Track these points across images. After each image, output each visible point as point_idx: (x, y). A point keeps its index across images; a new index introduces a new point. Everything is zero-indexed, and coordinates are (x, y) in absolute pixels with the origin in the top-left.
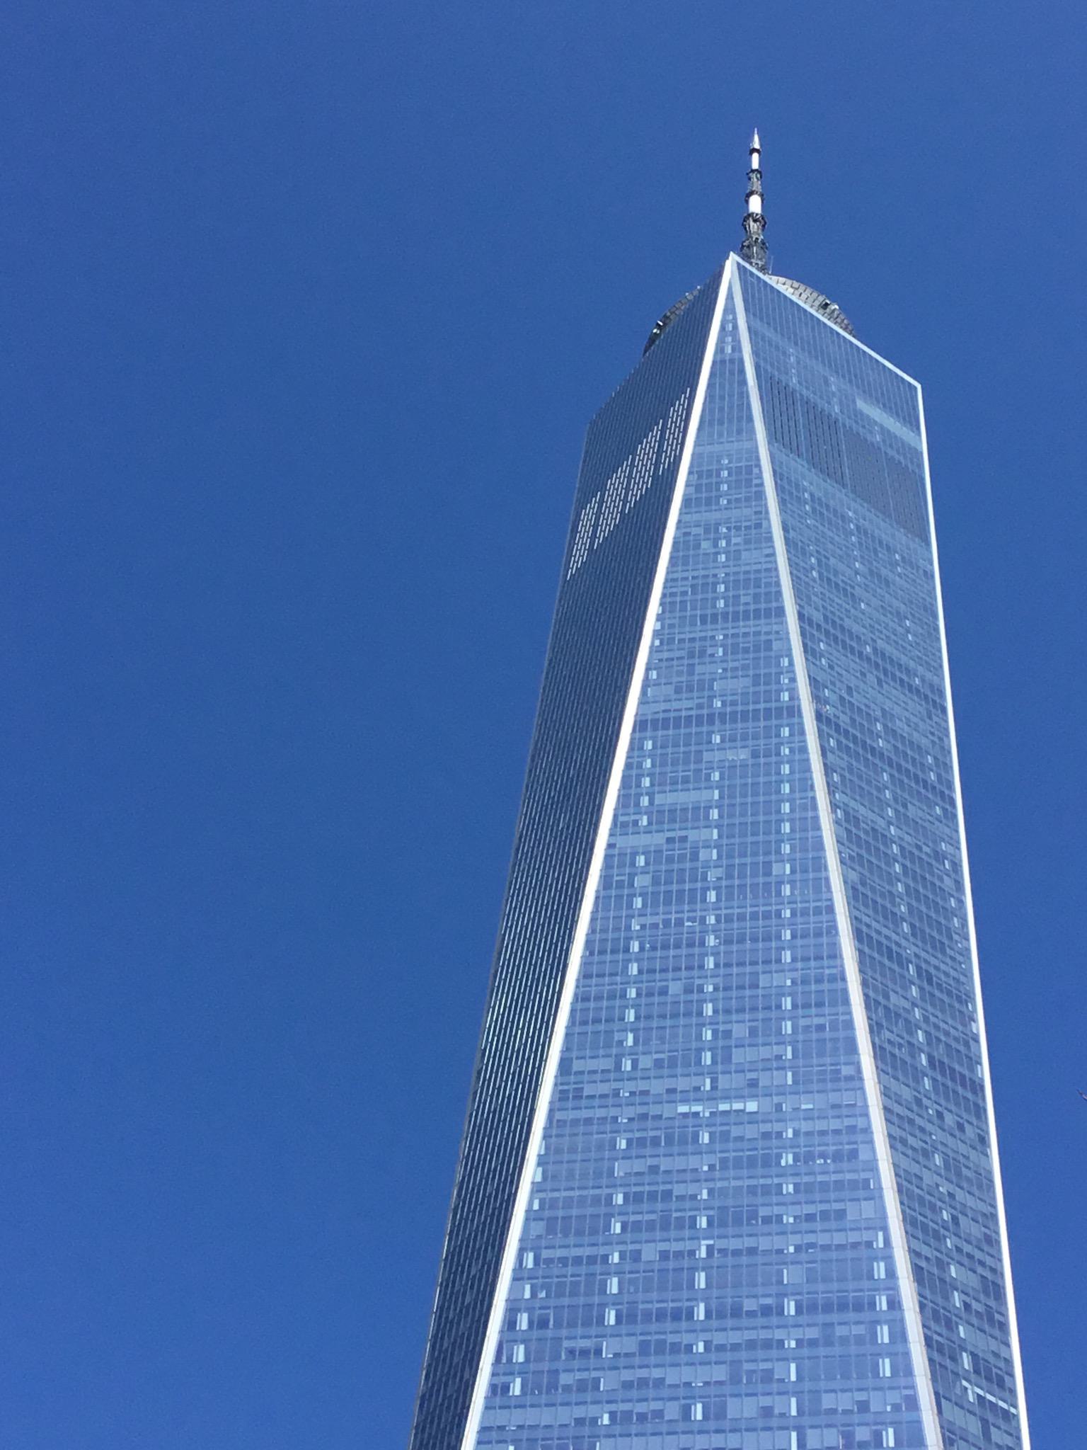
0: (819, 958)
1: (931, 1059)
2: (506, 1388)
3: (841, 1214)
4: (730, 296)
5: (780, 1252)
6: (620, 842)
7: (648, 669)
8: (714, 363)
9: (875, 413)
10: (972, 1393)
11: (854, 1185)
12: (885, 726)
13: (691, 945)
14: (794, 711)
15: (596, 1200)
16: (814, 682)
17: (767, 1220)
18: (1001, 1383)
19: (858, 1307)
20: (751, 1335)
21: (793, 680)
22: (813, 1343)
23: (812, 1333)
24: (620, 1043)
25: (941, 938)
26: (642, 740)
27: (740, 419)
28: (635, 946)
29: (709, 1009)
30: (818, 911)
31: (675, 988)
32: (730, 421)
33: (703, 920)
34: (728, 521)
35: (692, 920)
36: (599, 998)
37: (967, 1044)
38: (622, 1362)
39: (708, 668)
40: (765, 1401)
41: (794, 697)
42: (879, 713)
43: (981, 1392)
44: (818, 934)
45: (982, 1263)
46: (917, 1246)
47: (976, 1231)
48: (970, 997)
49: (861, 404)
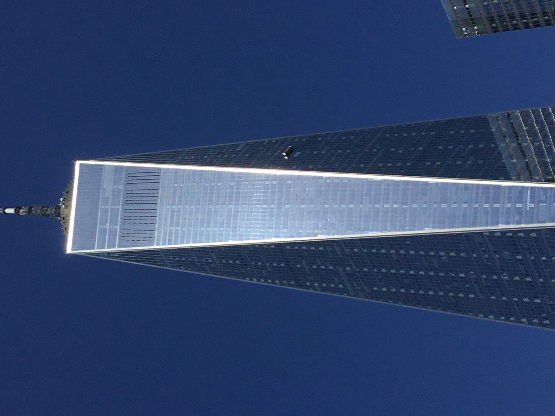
3: (480, 243)
7: (276, 284)
26: (306, 286)
30: (362, 243)
35: (377, 276)
43: (528, 202)
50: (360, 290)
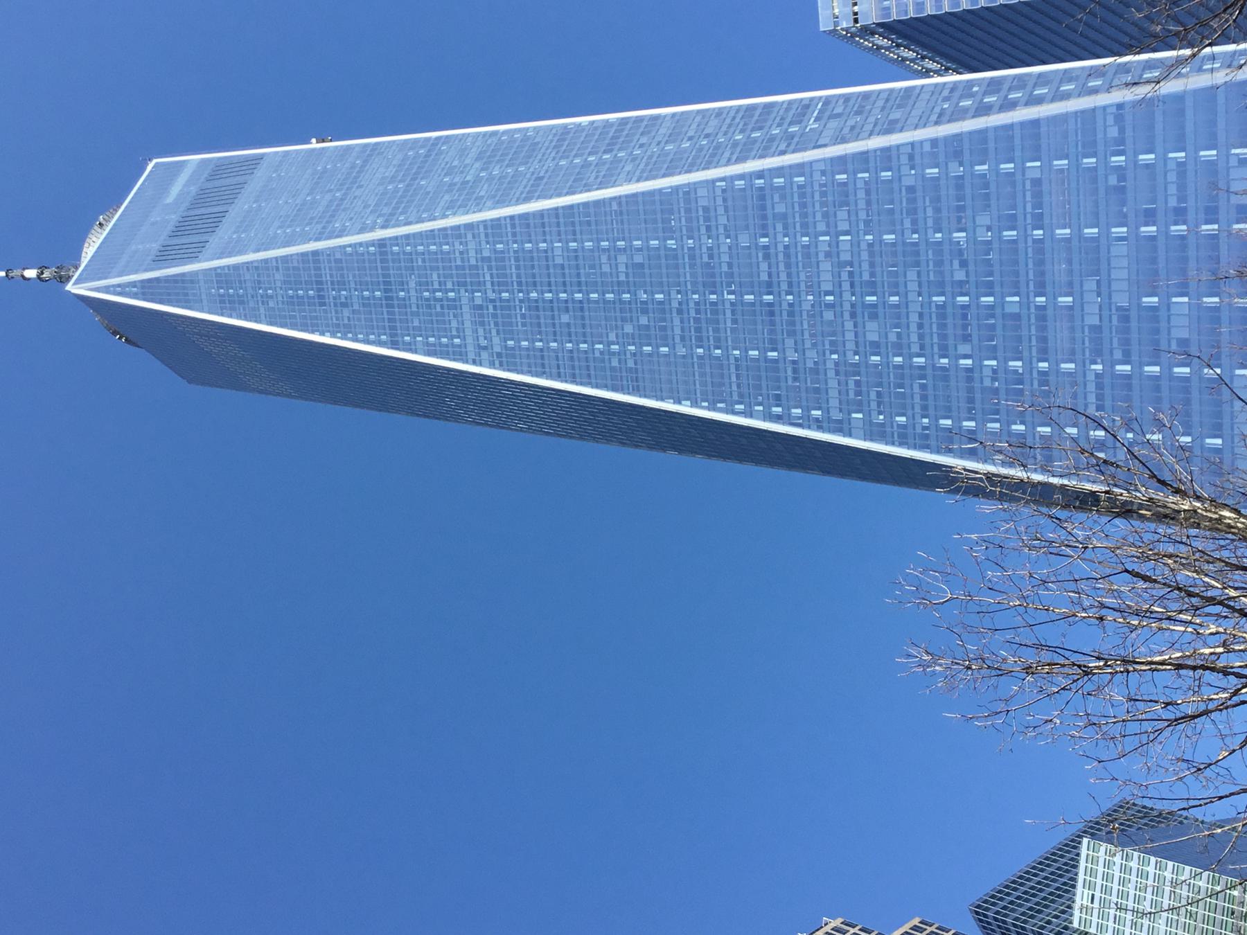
0: (543, 225)
1: (605, 152)
2: (817, 420)
3: (706, 209)
4: (97, 290)
5: (730, 248)
6: (471, 356)
8: (145, 300)
9: (175, 190)
10: (812, 125)
11: (687, 201)
12: (390, 183)
13: (537, 308)
14: (381, 243)
15: (701, 366)
16: (362, 230)
17: (711, 257)
18: (807, 107)
19: (762, 198)
20: (782, 267)
21: (361, 244)
22: (785, 227)
23: (779, 227)
24: (602, 353)
25: (529, 146)
27: (183, 281)
28: (539, 344)
29: (578, 296)
30: (513, 226)
31: (565, 318)
32: (184, 288)
33: (521, 301)
34: (254, 288)
36: (573, 368)
37: (596, 128)
38: (800, 347)
39: (355, 300)
40: (821, 256)
41: (372, 243)
42: (381, 188)
44: (528, 226)
45: (734, 118)
46: (723, 161)
47: (714, 123)
48: (565, 126)
49: (170, 200)
50: (485, 348)
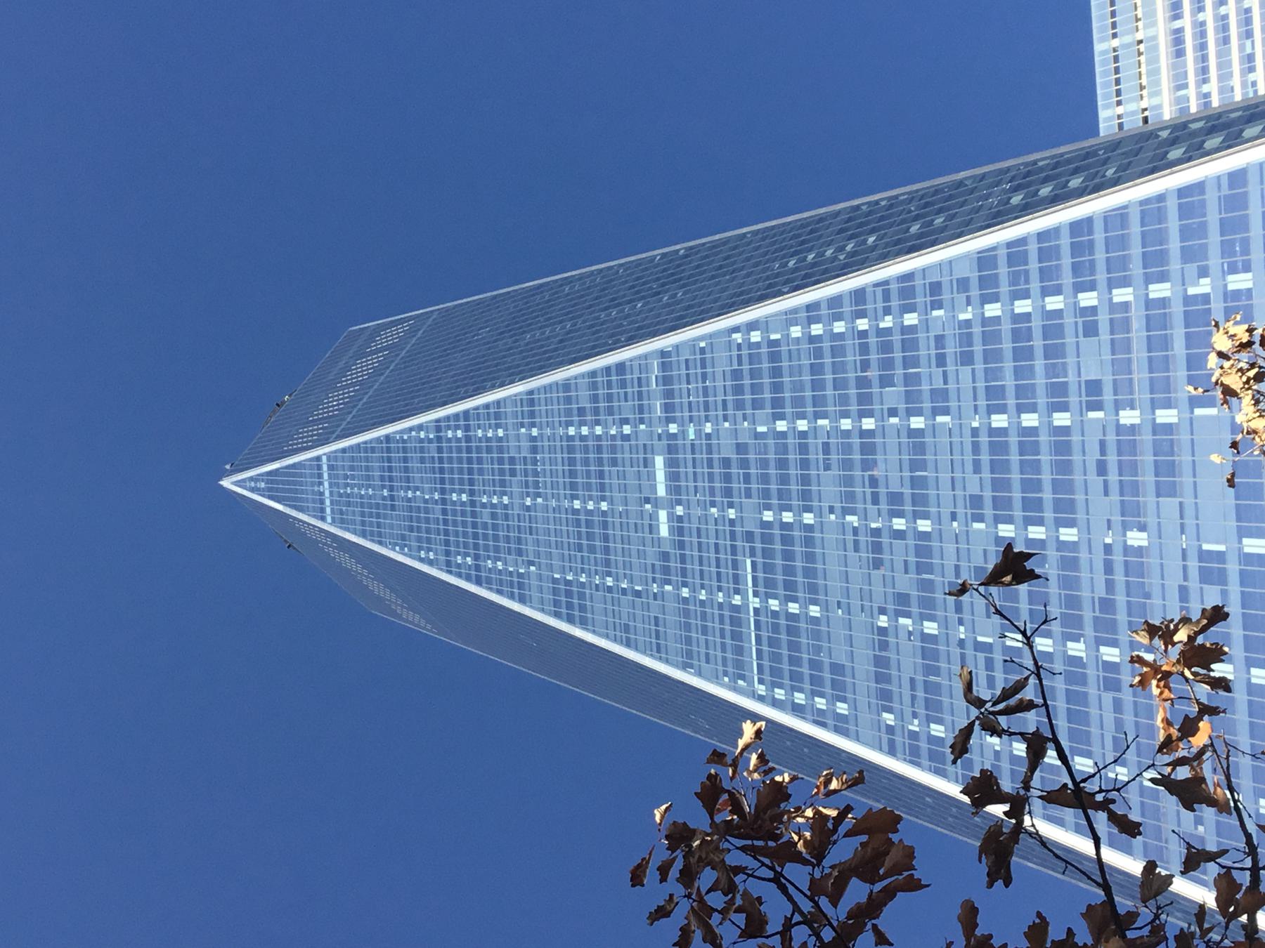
8: (271, 498)
14: (438, 425)
27: (294, 475)
32: (295, 483)
